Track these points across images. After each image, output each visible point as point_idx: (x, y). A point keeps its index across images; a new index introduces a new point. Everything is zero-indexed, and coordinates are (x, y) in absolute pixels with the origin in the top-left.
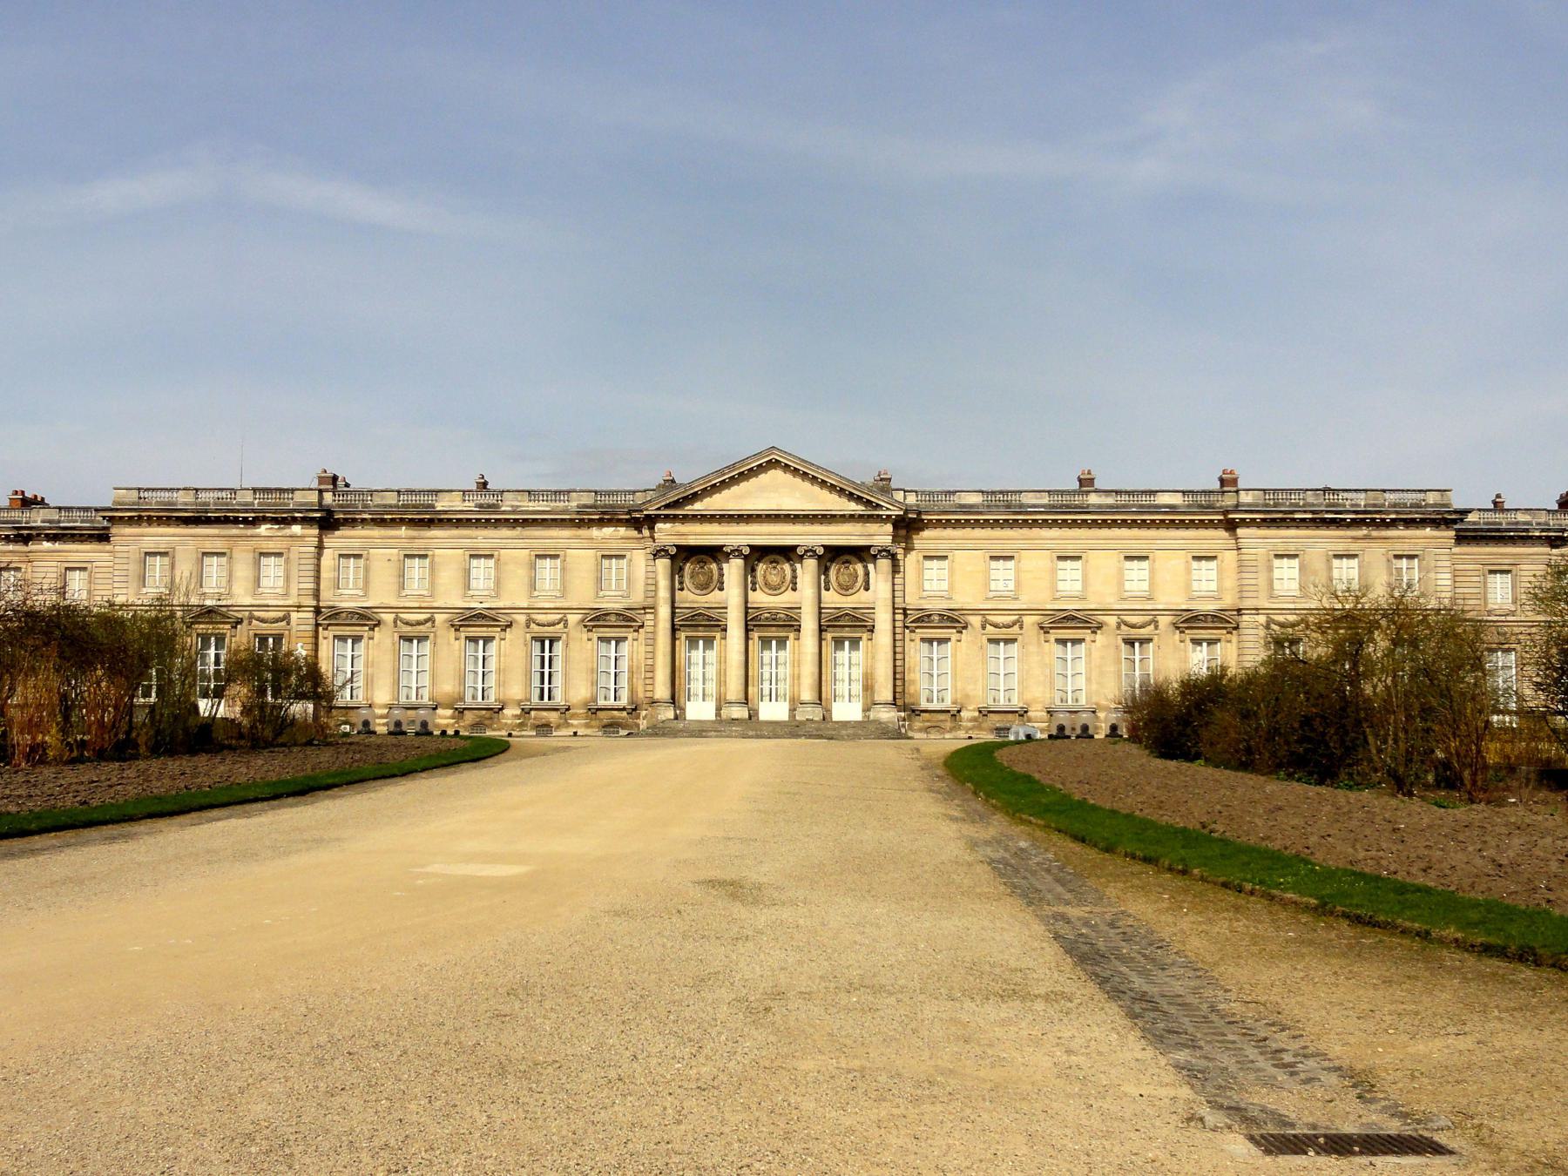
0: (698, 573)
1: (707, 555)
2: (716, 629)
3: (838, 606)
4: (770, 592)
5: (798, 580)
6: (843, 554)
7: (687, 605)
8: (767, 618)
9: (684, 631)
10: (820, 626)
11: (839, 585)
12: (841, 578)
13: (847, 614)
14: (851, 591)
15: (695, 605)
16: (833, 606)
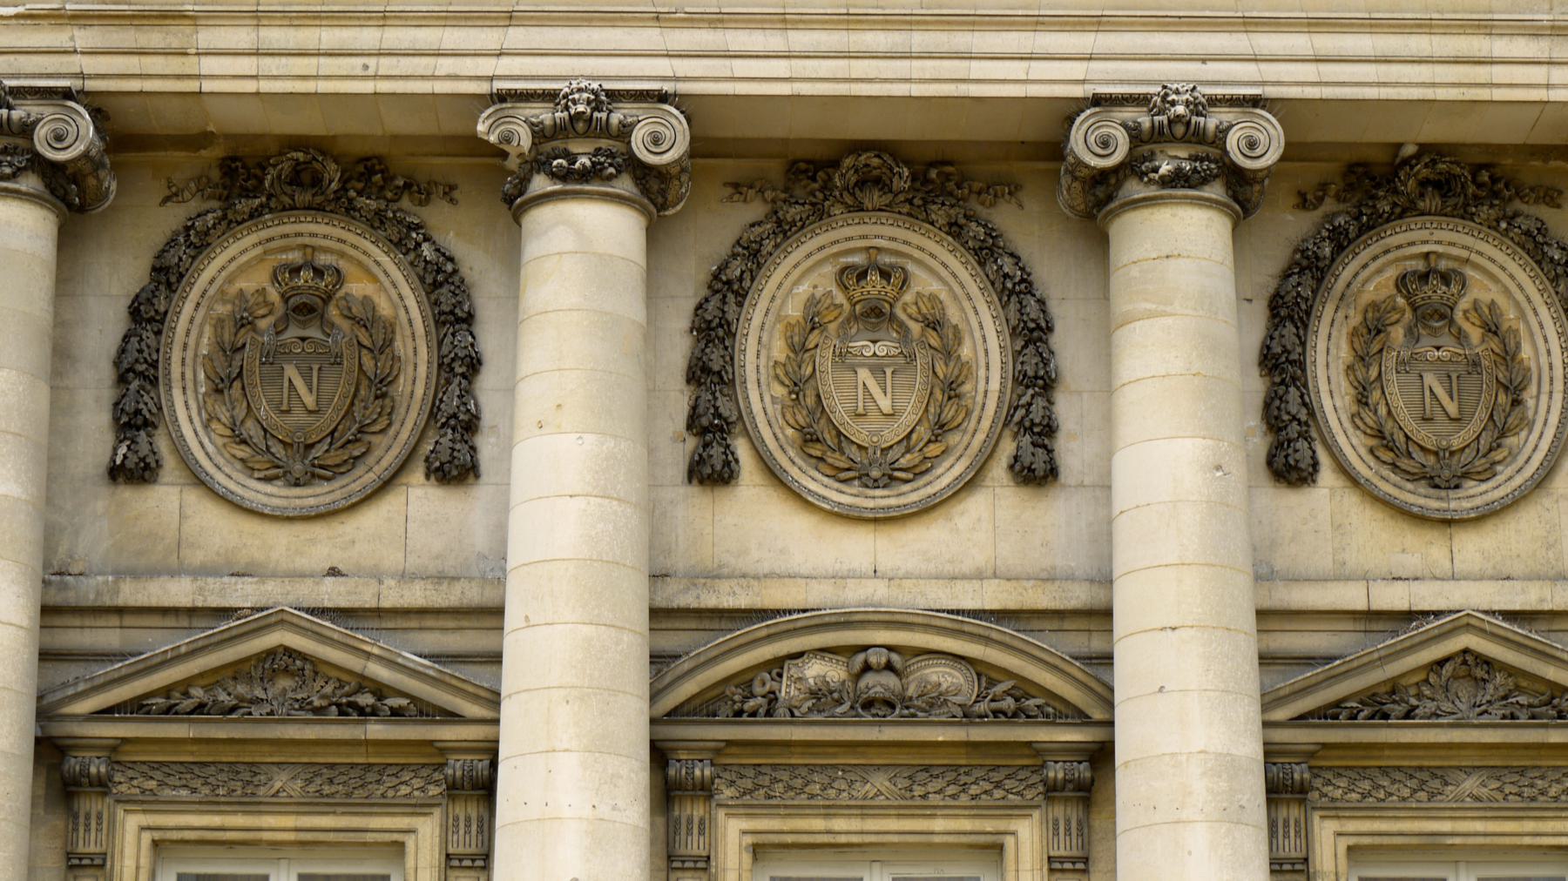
0: (273, 357)
1: (340, 206)
2: (410, 787)
3: (1393, 598)
4: (846, 497)
5: (1067, 409)
6: (1407, 210)
7: (179, 592)
8: (821, 696)
9: (146, 802)
10: (1271, 753)
11: (1385, 442)
12: (1398, 396)
13: (1474, 666)
14: (1475, 494)
15: (242, 594)
16: (1352, 597)
